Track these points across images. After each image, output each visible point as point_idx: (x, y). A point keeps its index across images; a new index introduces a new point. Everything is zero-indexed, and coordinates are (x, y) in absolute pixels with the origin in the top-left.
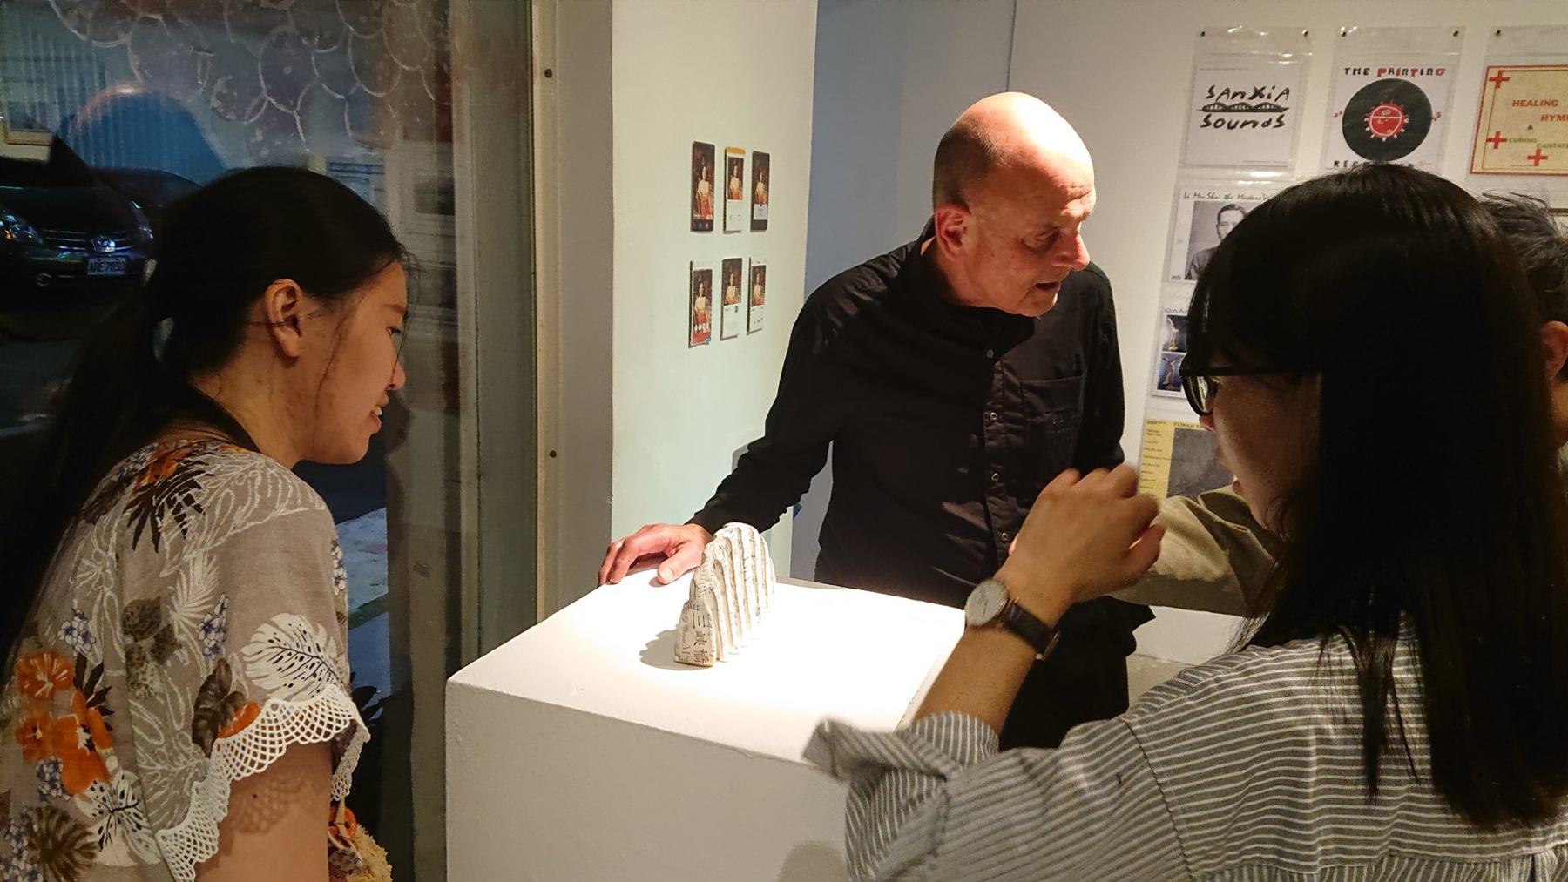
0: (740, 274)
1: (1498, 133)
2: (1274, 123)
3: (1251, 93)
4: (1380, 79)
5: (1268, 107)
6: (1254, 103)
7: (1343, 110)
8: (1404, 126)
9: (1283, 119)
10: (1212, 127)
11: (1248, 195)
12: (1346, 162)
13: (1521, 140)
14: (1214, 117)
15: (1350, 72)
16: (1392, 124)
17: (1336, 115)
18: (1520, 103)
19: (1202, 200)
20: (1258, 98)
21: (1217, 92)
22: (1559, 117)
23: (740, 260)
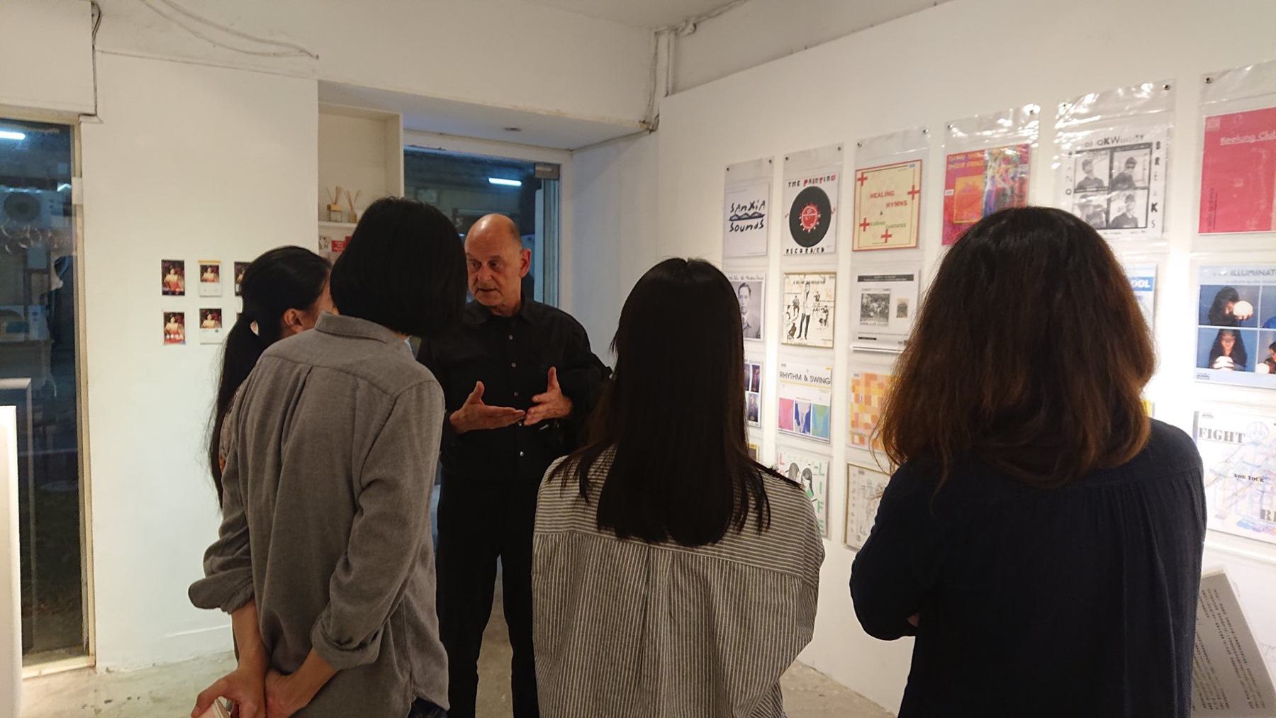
1: (865, 219)
2: (759, 226)
3: (748, 208)
4: (804, 188)
5: (756, 215)
6: (750, 213)
7: (789, 212)
9: (763, 222)
10: (734, 231)
11: (750, 277)
12: (792, 250)
13: (877, 223)
14: (736, 223)
15: (791, 184)
16: (811, 220)
18: (873, 196)
21: (735, 207)
22: (897, 204)
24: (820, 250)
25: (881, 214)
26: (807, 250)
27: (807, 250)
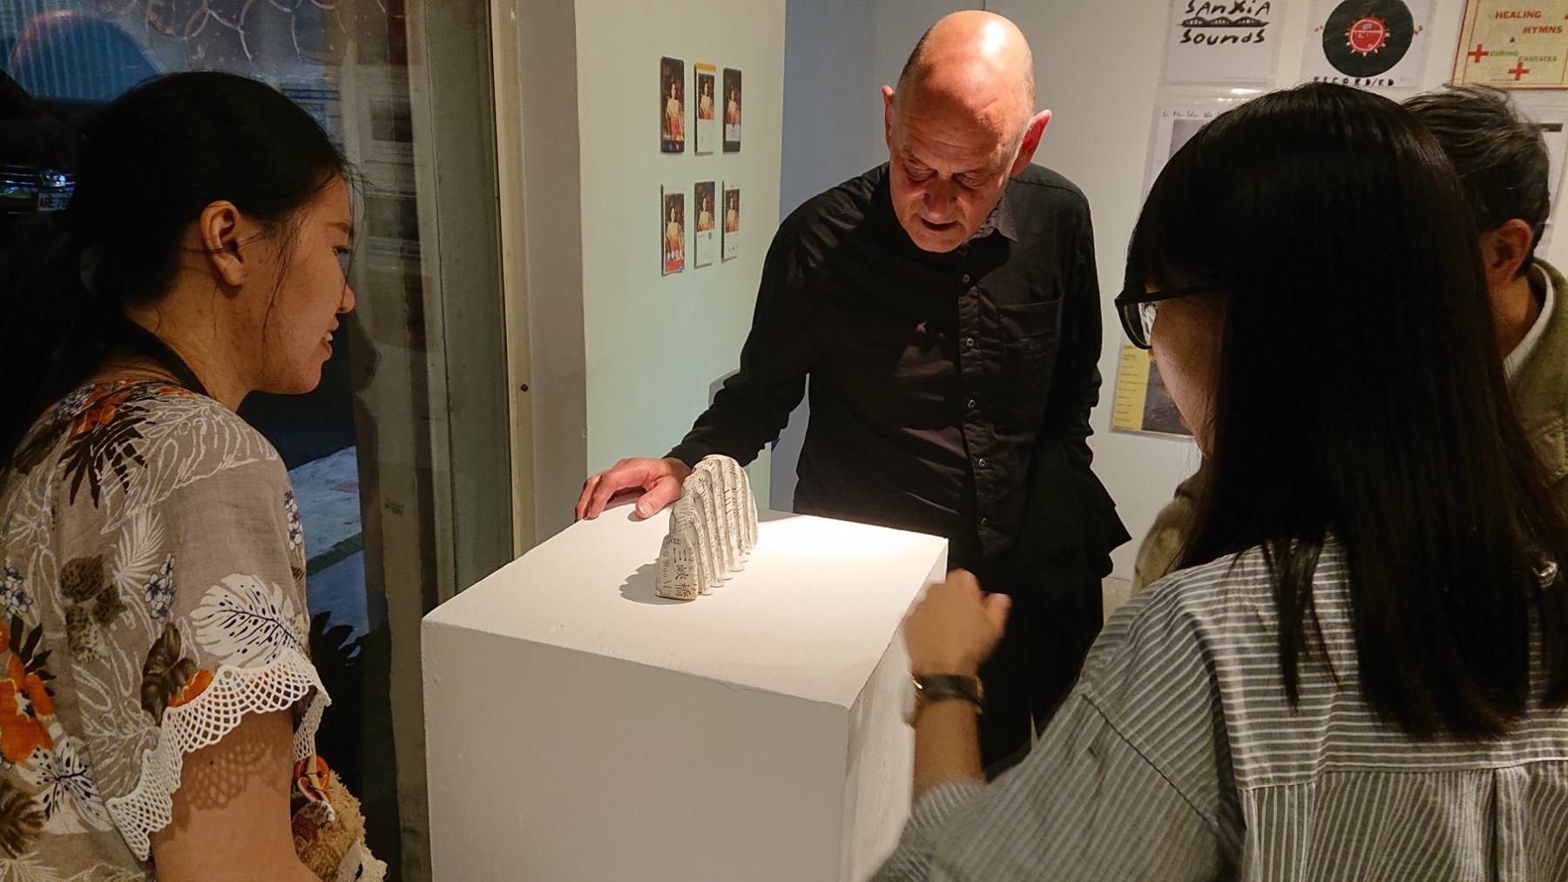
0: (713, 198)
1: (1480, 47)
2: (1254, 38)
3: (1230, 7)
5: (1248, 21)
6: (1237, 16)
7: (1324, 24)
8: (1386, 40)
9: (1263, 34)
10: (1192, 41)
13: (1502, 53)
14: (1194, 33)
16: (1370, 39)
17: (1317, 30)
18: (1503, 15)
19: (1181, 118)
20: (1238, 11)
21: (1197, 6)
22: (1543, 30)
23: (713, 184)
24: (1385, 83)
25: (1513, 40)
26: (1357, 81)
27: (1357, 81)
